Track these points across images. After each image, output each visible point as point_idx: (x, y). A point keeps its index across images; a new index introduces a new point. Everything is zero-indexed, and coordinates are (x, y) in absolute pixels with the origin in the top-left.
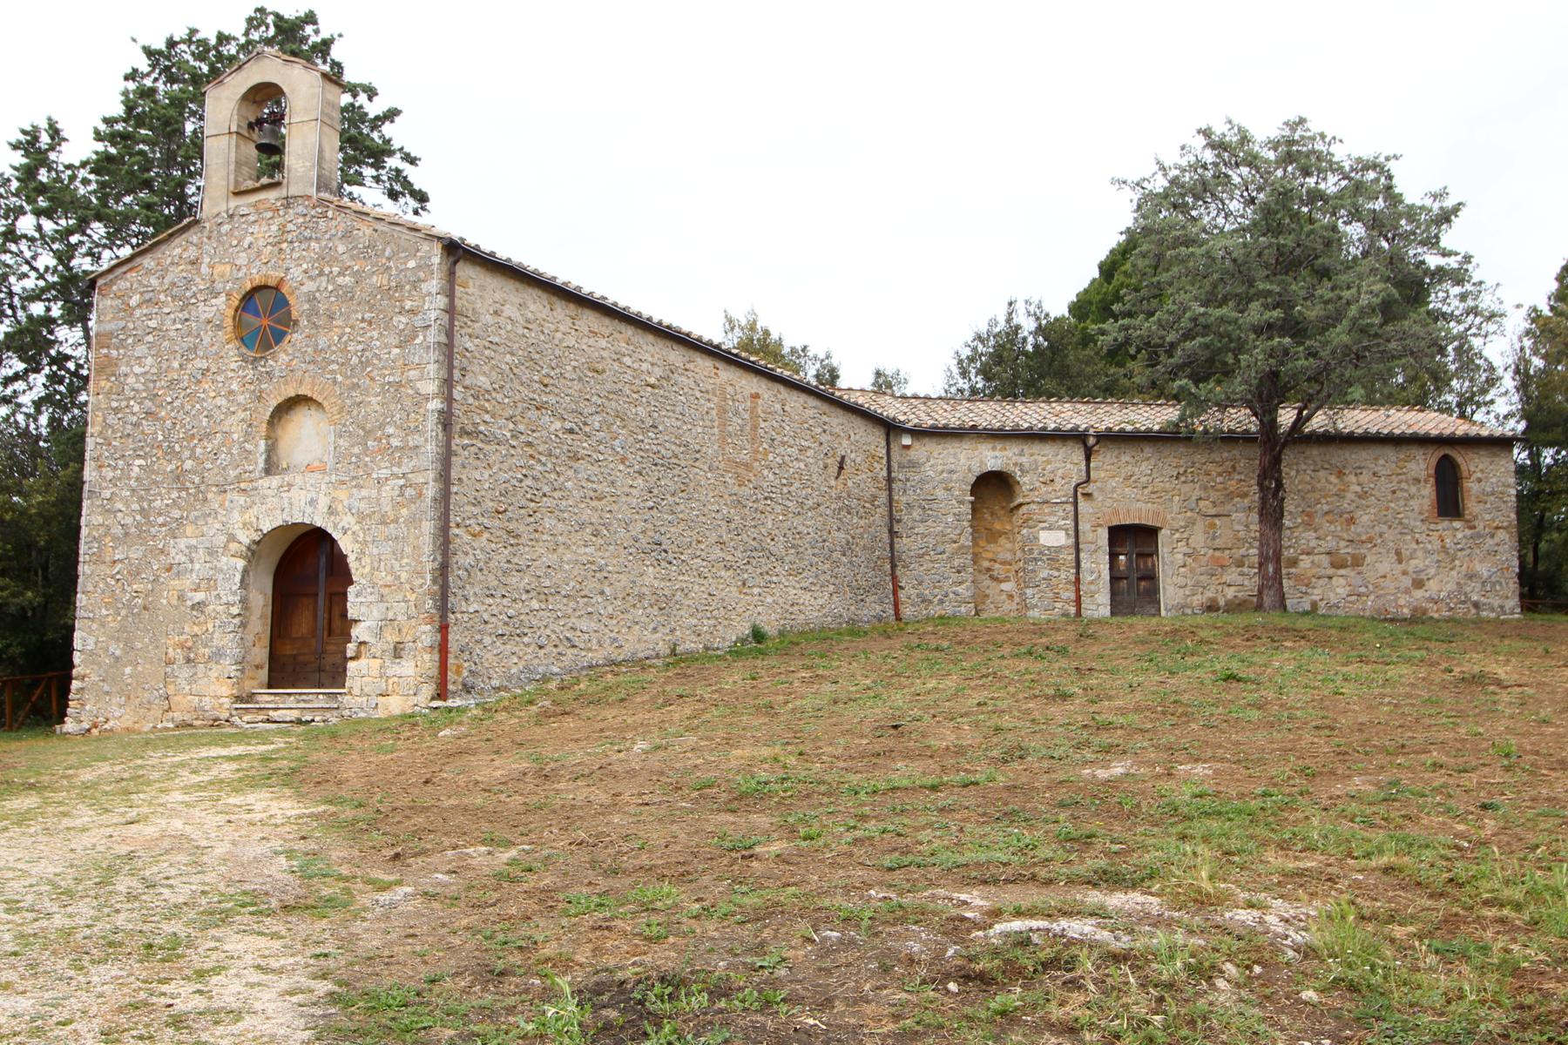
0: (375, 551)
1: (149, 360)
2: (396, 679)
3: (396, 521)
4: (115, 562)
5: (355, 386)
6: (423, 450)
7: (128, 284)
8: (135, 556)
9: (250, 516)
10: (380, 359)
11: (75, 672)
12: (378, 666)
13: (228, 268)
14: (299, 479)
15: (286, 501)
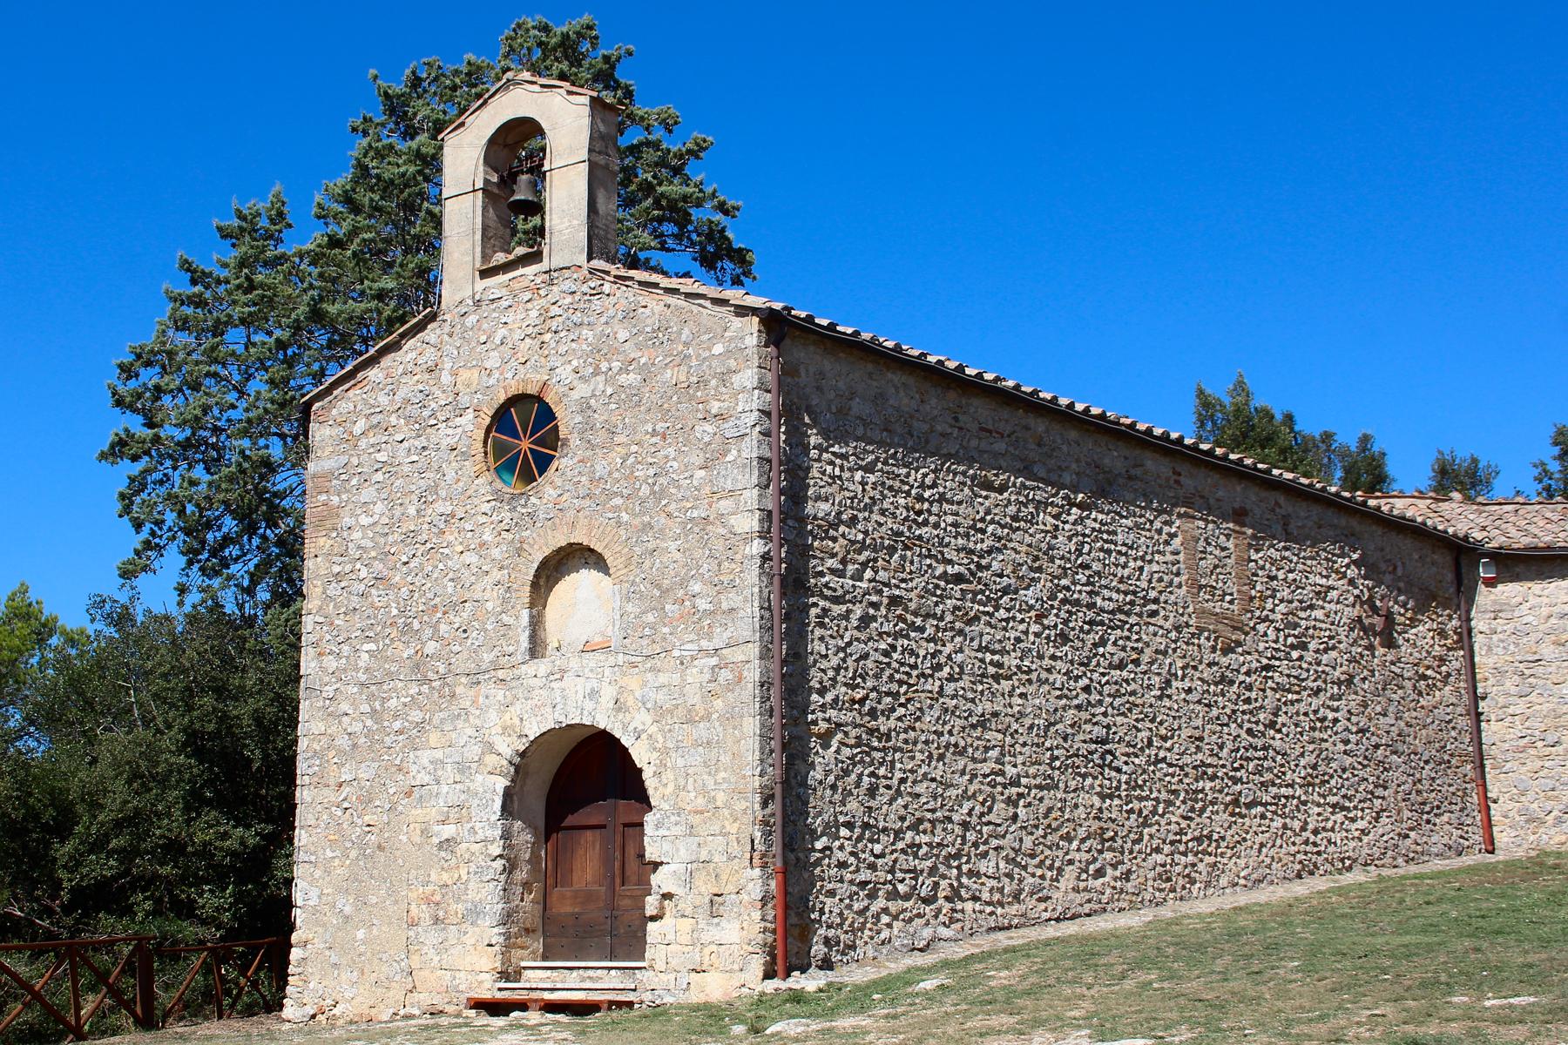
0: (680, 762)
1: (379, 507)
2: (714, 948)
3: (707, 717)
9: (511, 716)
10: (679, 487)
11: (294, 938)
13: (476, 372)
15: (558, 693)
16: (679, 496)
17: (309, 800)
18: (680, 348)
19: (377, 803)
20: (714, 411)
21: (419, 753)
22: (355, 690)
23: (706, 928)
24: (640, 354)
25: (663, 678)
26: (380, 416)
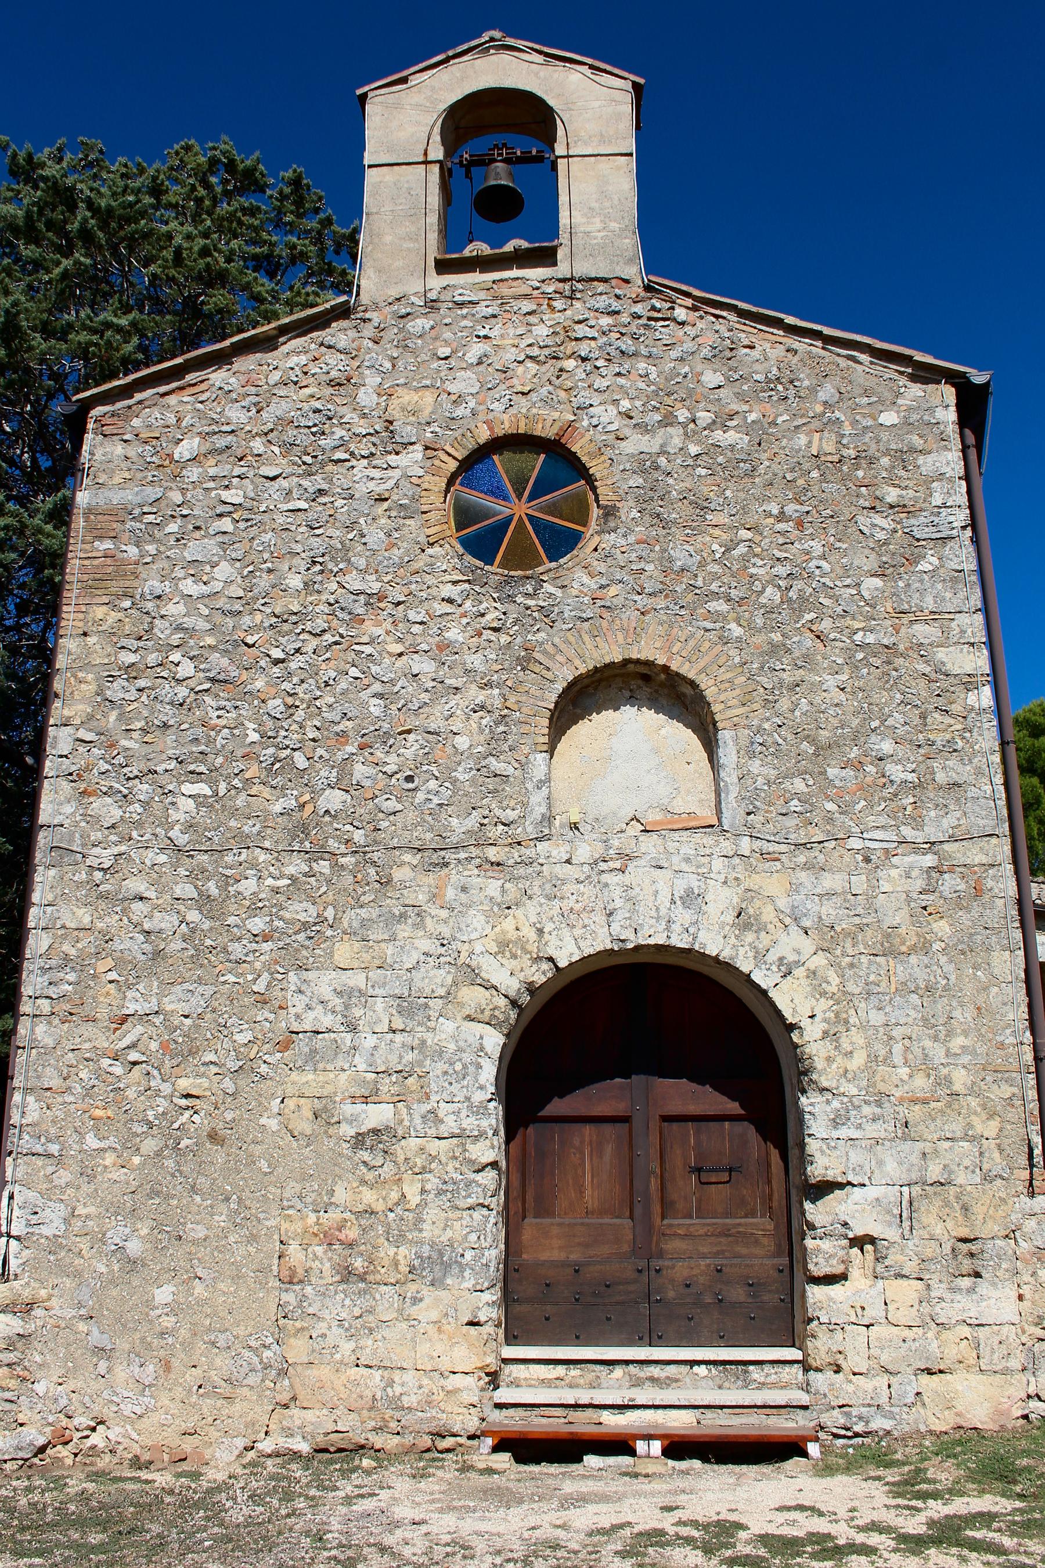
1: (224, 570)
4: (124, 1020)
5: (774, 649)
6: (972, 792)
7: (172, 419)
8: (183, 1008)
10: (837, 600)
12: (913, 1297)
13: (429, 398)
14: (650, 844)
15: (617, 893)
16: (839, 610)
17: (50, 1042)
18: (819, 409)
19: (211, 1057)
20: (889, 499)
21: (311, 975)
22: (162, 858)
23: (948, 1296)
24: (746, 408)
25: (830, 882)
26: (230, 438)
